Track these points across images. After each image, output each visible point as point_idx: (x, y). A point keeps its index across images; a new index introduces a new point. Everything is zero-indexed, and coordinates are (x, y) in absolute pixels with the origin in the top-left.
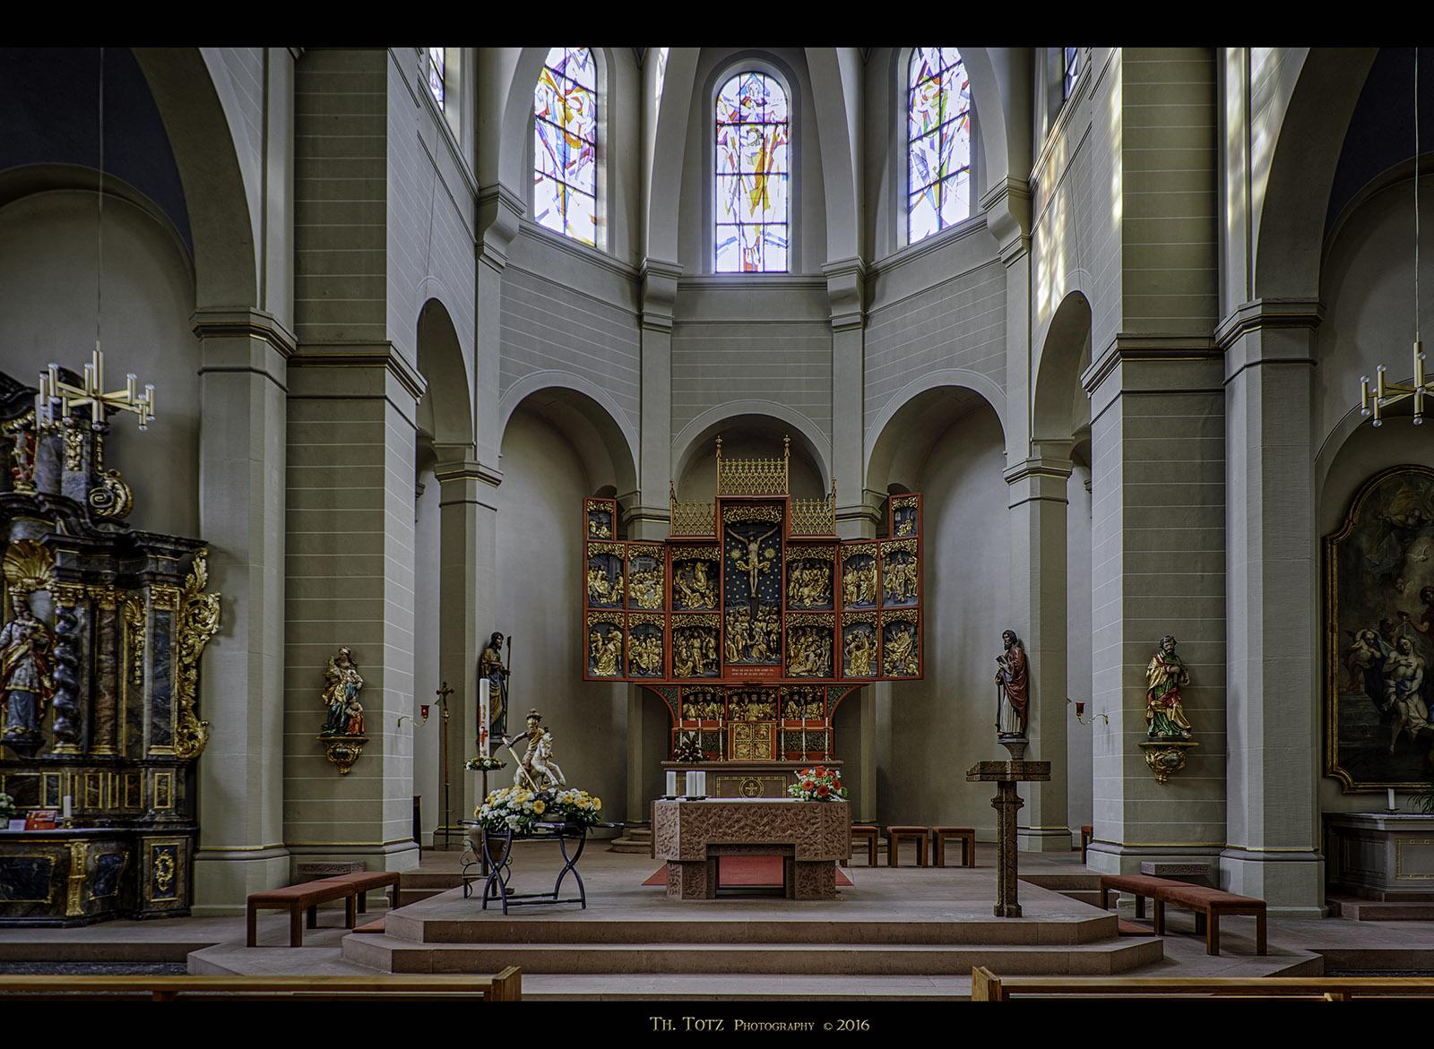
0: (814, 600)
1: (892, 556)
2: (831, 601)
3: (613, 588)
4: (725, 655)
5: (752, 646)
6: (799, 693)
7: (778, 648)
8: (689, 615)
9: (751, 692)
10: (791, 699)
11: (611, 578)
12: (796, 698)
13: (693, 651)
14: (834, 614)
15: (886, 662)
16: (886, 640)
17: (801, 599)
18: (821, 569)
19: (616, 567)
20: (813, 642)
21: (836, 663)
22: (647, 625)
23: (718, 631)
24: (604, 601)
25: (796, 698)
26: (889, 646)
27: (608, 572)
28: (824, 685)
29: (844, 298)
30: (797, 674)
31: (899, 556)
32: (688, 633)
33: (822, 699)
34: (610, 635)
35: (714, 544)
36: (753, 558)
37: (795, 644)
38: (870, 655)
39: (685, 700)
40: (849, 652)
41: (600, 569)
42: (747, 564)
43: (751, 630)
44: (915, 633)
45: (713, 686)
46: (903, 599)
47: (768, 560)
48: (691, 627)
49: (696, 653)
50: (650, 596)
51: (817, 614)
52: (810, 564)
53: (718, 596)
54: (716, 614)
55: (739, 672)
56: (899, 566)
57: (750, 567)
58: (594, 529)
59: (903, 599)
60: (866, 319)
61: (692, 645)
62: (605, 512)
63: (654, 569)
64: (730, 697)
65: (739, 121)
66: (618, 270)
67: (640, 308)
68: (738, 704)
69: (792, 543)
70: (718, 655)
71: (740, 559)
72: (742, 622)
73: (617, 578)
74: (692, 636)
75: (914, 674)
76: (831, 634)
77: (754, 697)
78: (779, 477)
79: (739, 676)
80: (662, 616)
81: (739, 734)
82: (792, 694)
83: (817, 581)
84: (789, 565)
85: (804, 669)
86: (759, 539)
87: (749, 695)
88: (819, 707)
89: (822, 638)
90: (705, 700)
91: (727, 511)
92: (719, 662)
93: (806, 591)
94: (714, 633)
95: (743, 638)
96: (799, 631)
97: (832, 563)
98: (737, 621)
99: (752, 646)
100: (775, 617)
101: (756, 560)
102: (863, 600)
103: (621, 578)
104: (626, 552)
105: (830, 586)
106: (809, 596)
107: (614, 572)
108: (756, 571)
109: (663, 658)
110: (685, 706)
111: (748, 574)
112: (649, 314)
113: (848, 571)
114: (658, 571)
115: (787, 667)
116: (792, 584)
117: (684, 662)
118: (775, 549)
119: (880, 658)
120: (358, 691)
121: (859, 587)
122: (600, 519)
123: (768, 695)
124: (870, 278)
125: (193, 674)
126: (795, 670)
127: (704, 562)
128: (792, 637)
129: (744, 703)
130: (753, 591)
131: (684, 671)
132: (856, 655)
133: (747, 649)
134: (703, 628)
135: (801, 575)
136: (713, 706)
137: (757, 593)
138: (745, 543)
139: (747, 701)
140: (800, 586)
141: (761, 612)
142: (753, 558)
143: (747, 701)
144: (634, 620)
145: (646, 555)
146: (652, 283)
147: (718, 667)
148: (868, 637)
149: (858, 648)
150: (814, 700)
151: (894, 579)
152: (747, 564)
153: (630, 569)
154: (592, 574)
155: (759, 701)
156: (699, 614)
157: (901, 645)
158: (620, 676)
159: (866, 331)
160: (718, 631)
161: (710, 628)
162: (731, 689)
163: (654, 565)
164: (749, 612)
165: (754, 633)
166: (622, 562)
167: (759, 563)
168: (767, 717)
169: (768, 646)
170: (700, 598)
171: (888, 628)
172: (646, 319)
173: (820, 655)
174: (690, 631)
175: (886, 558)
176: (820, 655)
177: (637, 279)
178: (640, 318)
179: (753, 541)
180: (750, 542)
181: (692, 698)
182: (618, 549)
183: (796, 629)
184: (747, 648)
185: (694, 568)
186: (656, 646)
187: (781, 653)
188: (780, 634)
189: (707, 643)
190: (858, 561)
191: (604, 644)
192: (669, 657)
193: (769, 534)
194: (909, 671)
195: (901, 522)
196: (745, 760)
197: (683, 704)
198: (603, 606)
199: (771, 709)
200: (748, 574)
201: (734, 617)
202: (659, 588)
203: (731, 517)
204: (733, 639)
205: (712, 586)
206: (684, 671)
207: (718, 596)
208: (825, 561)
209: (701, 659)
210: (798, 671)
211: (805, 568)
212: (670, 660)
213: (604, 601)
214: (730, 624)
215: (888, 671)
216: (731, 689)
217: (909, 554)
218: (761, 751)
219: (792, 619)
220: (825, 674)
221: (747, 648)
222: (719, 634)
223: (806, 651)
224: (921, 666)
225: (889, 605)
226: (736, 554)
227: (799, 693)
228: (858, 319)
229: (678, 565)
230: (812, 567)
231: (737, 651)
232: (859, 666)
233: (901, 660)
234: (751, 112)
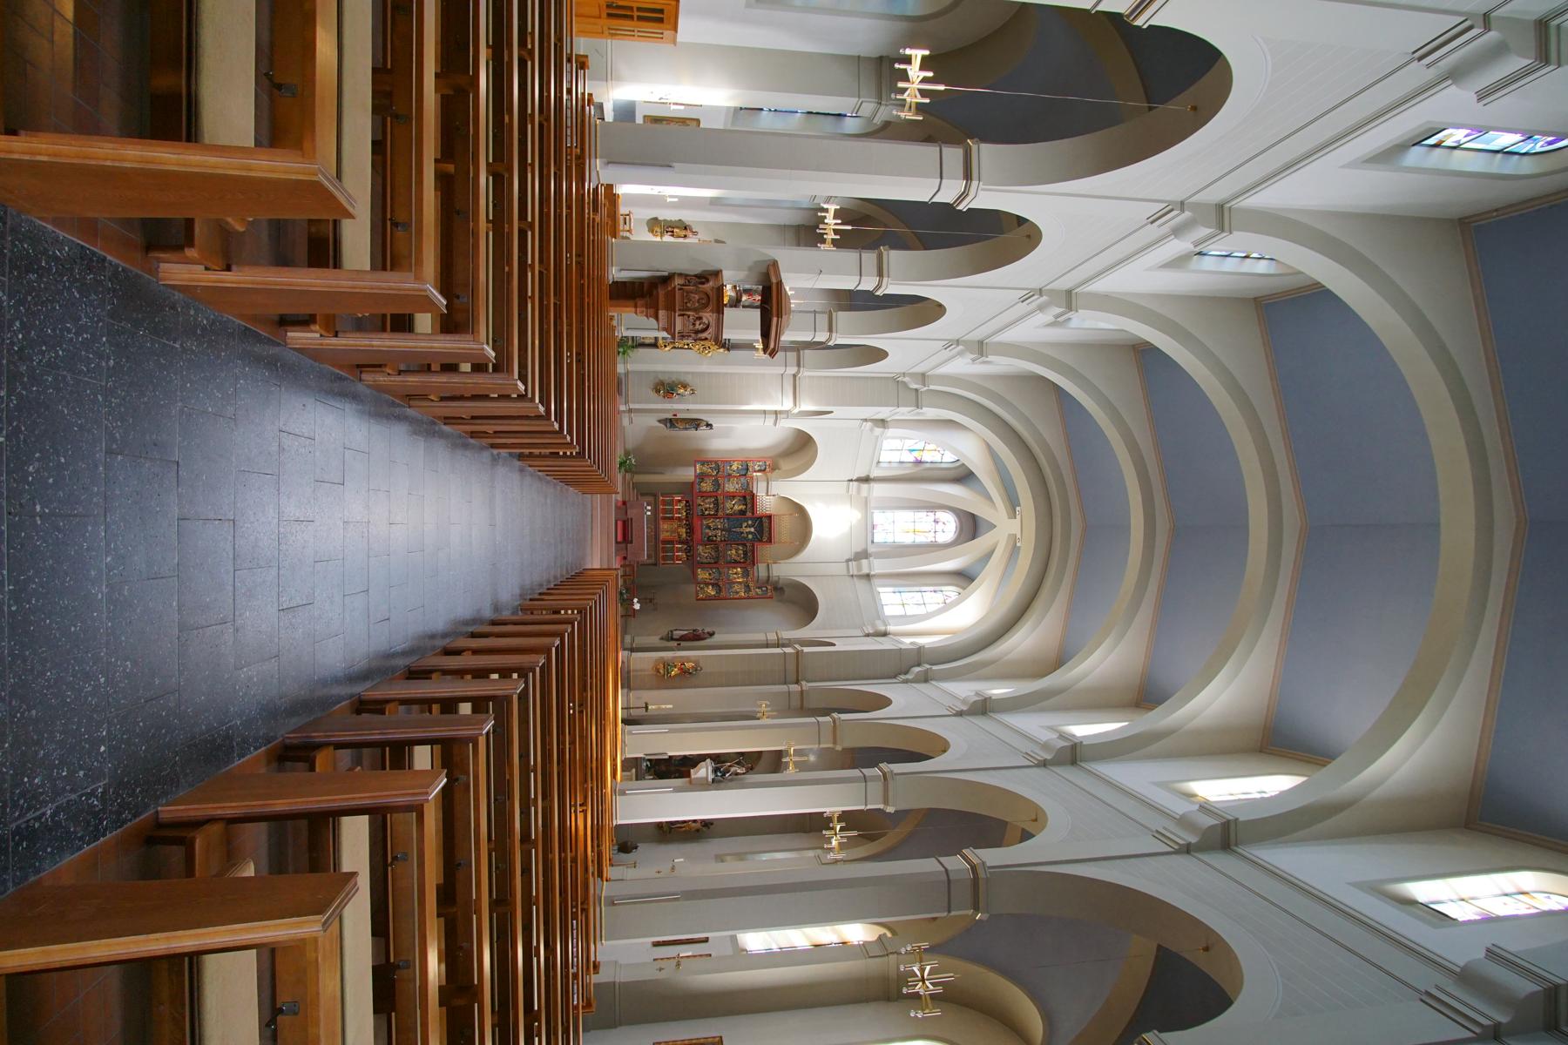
2: (730, 563)
7: (710, 540)
9: (691, 530)
13: (708, 504)
16: (713, 585)
21: (702, 565)
22: (719, 485)
29: (859, 568)
35: (753, 513)
36: (748, 530)
39: (687, 502)
50: (731, 487)
52: (745, 553)
65: (936, 522)
66: (870, 471)
67: (856, 480)
69: (753, 546)
76: (715, 563)
93: (734, 552)
96: (717, 549)
105: (736, 562)
109: (705, 492)
111: (741, 527)
117: (703, 501)
120: (683, 395)
121: (736, 574)
124: (868, 576)
125: (686, 347)
126: (700, 548)
131: (699, 501)
142: (748, 530)
145: (748, 484)
146: (865, 486)
149: (710, 574)
153: (742, 479)
155: (686, 533)
157: (711, 591)
166: (745, 475)
171: (717, 585)
172: (851, 483)
174: (716, 503)
177: (866, 480)
178: (851, 480)
184: (709, 527)
190: (746, 574)
203: (764, 520)
206: (699, 501)
212: (704, 495)
221: (709, 527)
222: (715, 516)
224: (702, 599)
226: (750, 522)
228: (851, 573)
229: (744, 497)
232: (702, 575)
234: (939, 527)
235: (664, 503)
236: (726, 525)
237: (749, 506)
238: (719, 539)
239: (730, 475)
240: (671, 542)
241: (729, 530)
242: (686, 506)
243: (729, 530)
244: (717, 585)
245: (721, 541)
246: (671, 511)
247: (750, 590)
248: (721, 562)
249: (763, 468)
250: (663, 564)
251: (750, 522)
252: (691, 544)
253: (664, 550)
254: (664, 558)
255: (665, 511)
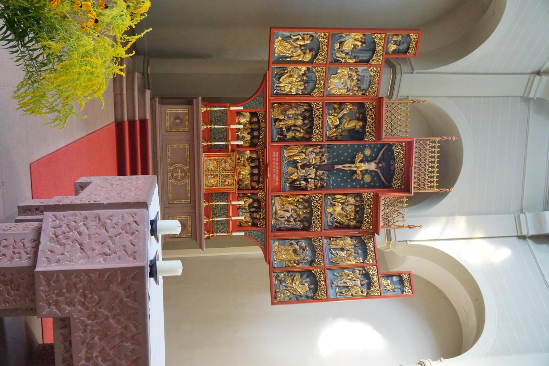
0: (332, 215)
1: (367, 276)
3: (347, 54)
4: (289, 146)
5: (296, 167)
6: (259, 207)
7: (295, 187)
8: (322, 116)
10: (255, 201)
11: (354, 53)
12: (256, 205)
14: (321, 231)
15: (285, 275)
16: (302, 272)
17: (333, 205)
18: (355, 219)
19: (364, 56)
20: (299, 215)
23: (309, 140)
24: (337, 46)
25: (256, 205)
26: (298, 276)
27: (360, 50)
28: (266, 227)
30: (274, 203)
31: (366, 281)
32: (307, 114)
33: (254, 225)
34: (308, 51)
36: (365, 166)
37: (298, 201)
38: (290, 261)
39: (253, 114)
40: (291, 244)
41: (363, 43)
42: (359, 162)
43: (309, 166)
44: (308, 297)
45: (265, 137)
46: (333, 286)
47: (363, 177)
48: (311, 117)
49: (291, 122)
51: (321, 219)
52: (359, 210)
53: (336, 139)
54: (323, 138)
55: (276, 157)
56: (359, 282)
57: (358, 164)
58: (395, 38)
59: (333, 286)
60: (523, 237)
61: (297, 119)
62: (408, 48)
63: (359, 88)
64: (256, 152)
68: (250, 157)
69: (376, 198)
70: (289, 140)
71: (364, 156)
72: (315, 159)
73: (355, 58)
74: (304, 118)
75: (276, 298)
76: (306, 229)
77: (256, 171)
78: (424, 185)
79: (273, 157)
80: (322, 94)
81: (225, 162)
82: (258, 201)
83: (346, 216)
84: (359, 195)
85: (278, 209)
86: (378, 171)
87: (258, 167)
88: (247, 222)
89: (301, 221)
90: (253, 130)
91: (402, 146)
92: (284, 140)
93: (338, 209)
94: (307, 136)
95: (301, 160)
97: (360, 227)
98: (317, 154)
99: (296, 167)
100: (319, 184)
101: (363, 168)
102: (332, 253)
103: (355, 60)
104: (376, 66)
105: (341, 226)
106: (335, 211)
107: (360, 55)
108: (355, 169)
109: (287, 95)
110: (248, 114)
111: (353, 162)
112: (540, 81)
113: (354, 240)
114: (357, 91)
115: (279, 196)
116: (344, 197)
117: (284, 112)
118: (371, 182)
119: (288, 270)
121: (342, 249)
122: (403, 43)
123: (258, 182)
127: (364, 127)
128: (302, 198)
129: (251, 162)
130: (340, 167)
132: (289, 250)
133: (293, 164)
134: (311, 127)
135: (350, 204)
136: (249, 137)
137: (338, 169)
138: (375, 159)
139: (252, 165)
140: (342, 204)
141: (323, 173)
142: (365, 166)
143: (252, 165)
144: (318, 73)
147: (280, 140)
148: (304, 259)
149: (295, 251)
150: (253, 218)
151: (349, 278)
152: (359, 162)
154: (359, 36)
155: (252, 174)
156: (323, 124)
158: (273, 60)
159: (515, 238)
160: (309, 140)
161: (311, 133)
162: (263, 153)
163: (364, 86)
164: (323, 163)
165: (307, 168)
166: (367, 62)
167: (360, 171)
168: (240, 182)
169: (296, 180)
170: (335, 124)
171: (310, 274)
173: (288, 221)
175: (365, 270)
176: (289, 222)
179: (378, 166)
180: (378, 164)
181: (255, 120)
182: (378, 59)
183: (309, 201)
185: (358, 119)
186: (297, 89)
187: (290, 191)
188: (307, 188)
189: (298, 131)
191: (301, 46)
192: (288, 100)
193: (383, 178)
194: (278, 295)
195: (392, 281)
196: (204, 167)
197: (250, 113)
198: (333, 45)
199: (246, 185)
200: (353, 162)
201: (320, 152)
202: (344, 91)
204: (302, 152)
205: (344, 134)
206: (275, 113)
207: (336, 139)
208: (361, 222)
209: (286, 126)
210: (276, 204)
211: (356, 206)
213: (337, 46)
214: (314, 149)
215: (277, 277)
216: (263, 153)
217: (369, 288)
218: (212, 181)
219: (317, 197)
220: (273, 226)
223: (292, 210)
225: (329, 274)
226: (368, 152)
227: (259, 207)
228: (525, 233)
229: (361, 105)
230: (357, 212)
231: (292, 156)
233: (286, 287)
235: (209, 118)
236: (324, 158)
237: (369, 120)
238: (311, 185)
239: (337, 61)
240: (224, 195)
241: (329, 168)
242: (251, 123)
243: (329, 168)
244: (310, 274)
245: (316, 189)
246: (223, 135)
247: (369, 285)
248: (316, 228)
249: (403, 47)
250: (208, 238)
251: (368, 152)
252: (261, 196)
253: (210, 212)
254: (210, 228)
255: (209, 135)
